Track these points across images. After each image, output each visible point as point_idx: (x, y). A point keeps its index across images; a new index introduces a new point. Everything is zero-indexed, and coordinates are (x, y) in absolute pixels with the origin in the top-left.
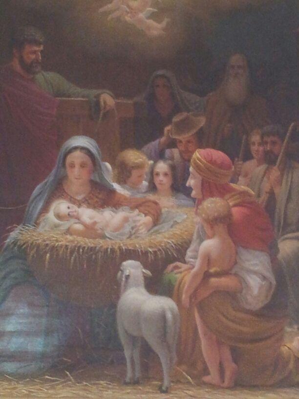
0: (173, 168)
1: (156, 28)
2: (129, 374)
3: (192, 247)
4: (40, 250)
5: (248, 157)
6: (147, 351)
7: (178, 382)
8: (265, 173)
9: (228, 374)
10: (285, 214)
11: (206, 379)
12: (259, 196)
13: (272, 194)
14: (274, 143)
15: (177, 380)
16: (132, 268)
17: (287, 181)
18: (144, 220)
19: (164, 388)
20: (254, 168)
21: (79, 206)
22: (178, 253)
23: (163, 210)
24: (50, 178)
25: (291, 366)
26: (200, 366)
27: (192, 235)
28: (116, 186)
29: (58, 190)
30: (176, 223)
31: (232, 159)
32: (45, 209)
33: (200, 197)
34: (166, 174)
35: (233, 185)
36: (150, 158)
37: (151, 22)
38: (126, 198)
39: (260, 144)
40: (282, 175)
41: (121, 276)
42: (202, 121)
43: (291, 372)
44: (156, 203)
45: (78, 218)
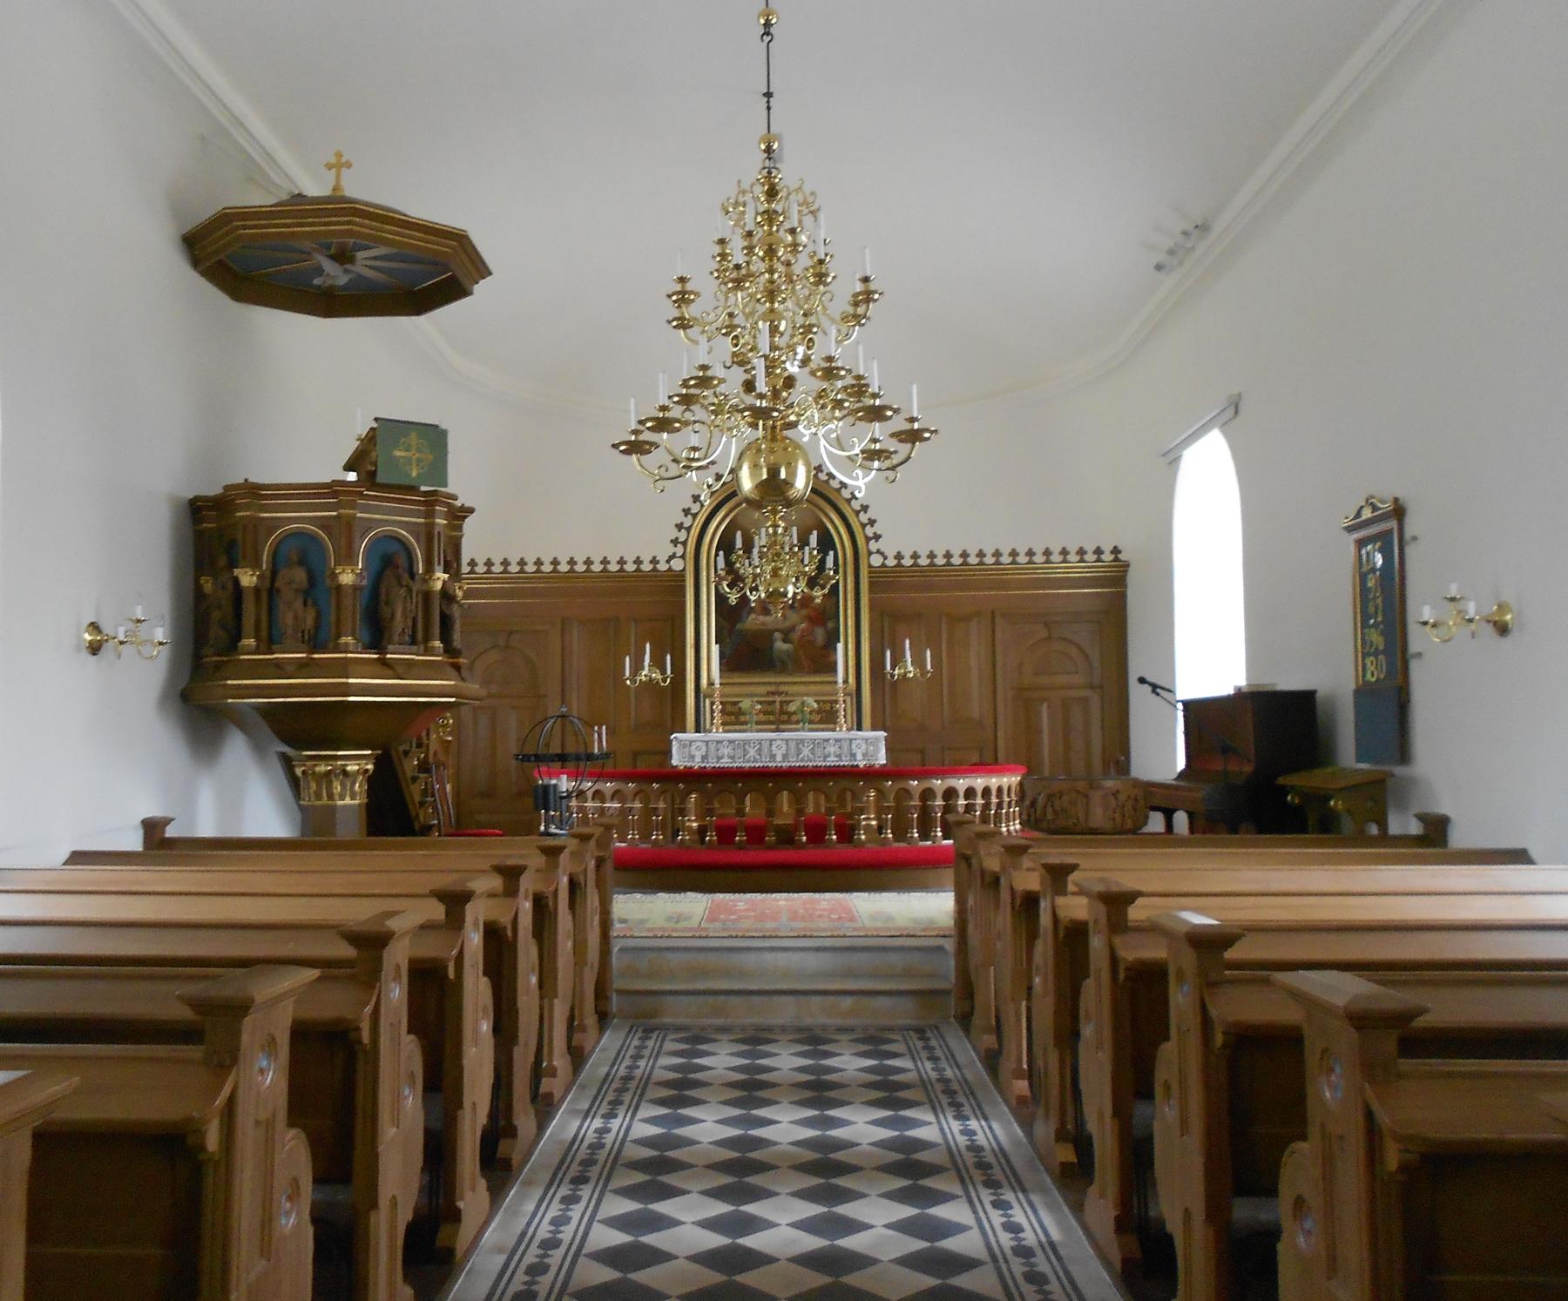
6: (783, 662)
16: (777, 635)
32: (748, 617)
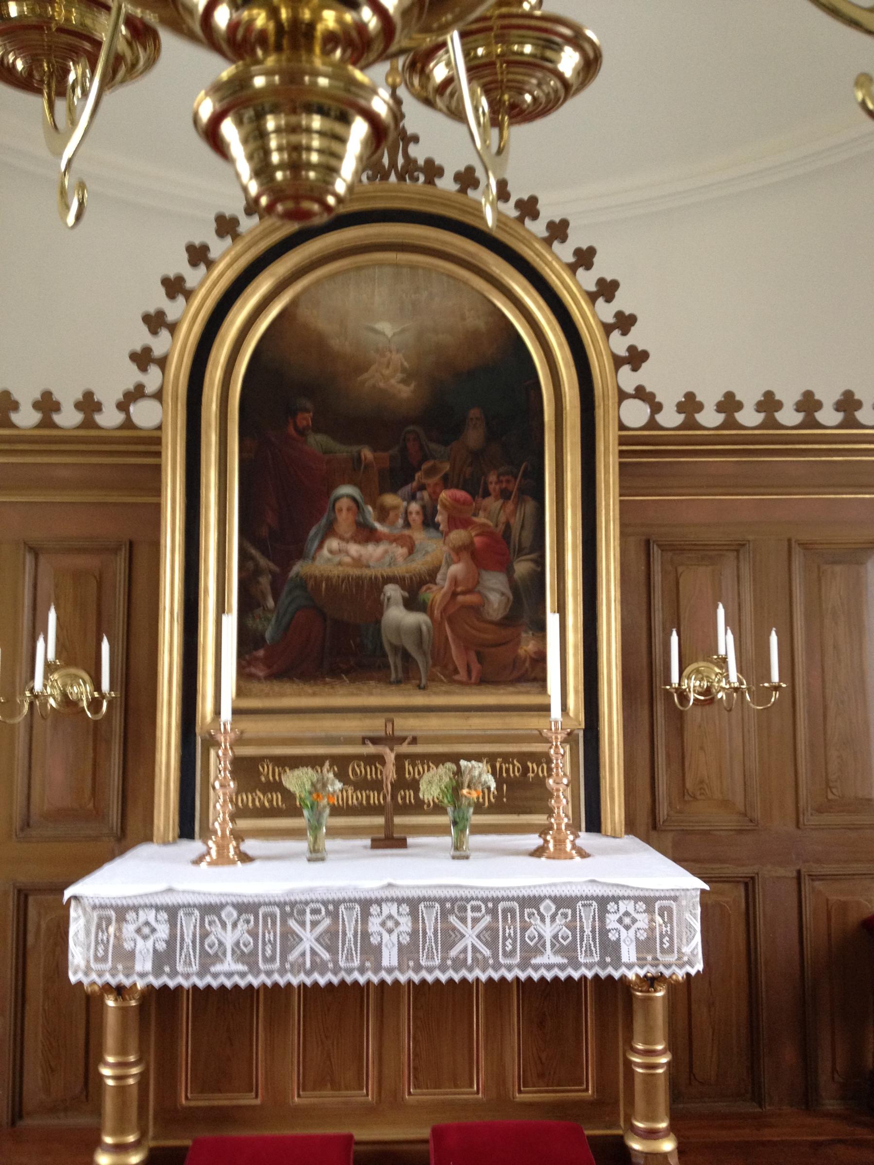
0: (424, 507)
1: (405, 391)
2: (393, 676)
3: (442, 571)
4: (317, 581)
5: (486, 494)
6: (406, 656)
7: (433, 680)
8: (501, 506)
9: (474, 674)
10: (520, 539)
11: (457, 677)
12: (497, 526)
13: (508, 526)
14: (508, 481)
15: (432, 679)
16: (392, 591)
17: (520, 514)
18: (400, 551)
19: (422, 685)
20: (493, 504)
21: (348, 542)
22: (431, 576)
23: (416, 543)
24: (323, 521)
25: (527, 664)
26: (451, 667)
27: (441, 562)
28: (378, 525)
29: (330, 531)
30: (427, 553)
31: (473, 494)
32: (321, 546)
33: (447, 529)
34: (418, 513)
35: (475, 519)
36: (404, 499)
37: (402, 387)
38: (384, 534)
39: (496, 483)
40: (516, 509)
41: (384, 599)
42: (447, 467)
43: (527, 671)
44: (410, 537)
45: (347, 553)
